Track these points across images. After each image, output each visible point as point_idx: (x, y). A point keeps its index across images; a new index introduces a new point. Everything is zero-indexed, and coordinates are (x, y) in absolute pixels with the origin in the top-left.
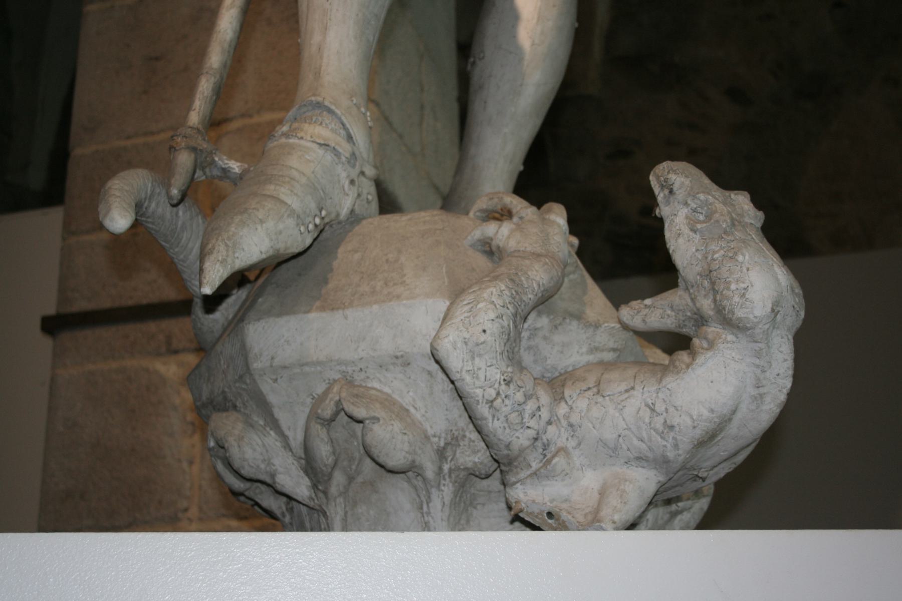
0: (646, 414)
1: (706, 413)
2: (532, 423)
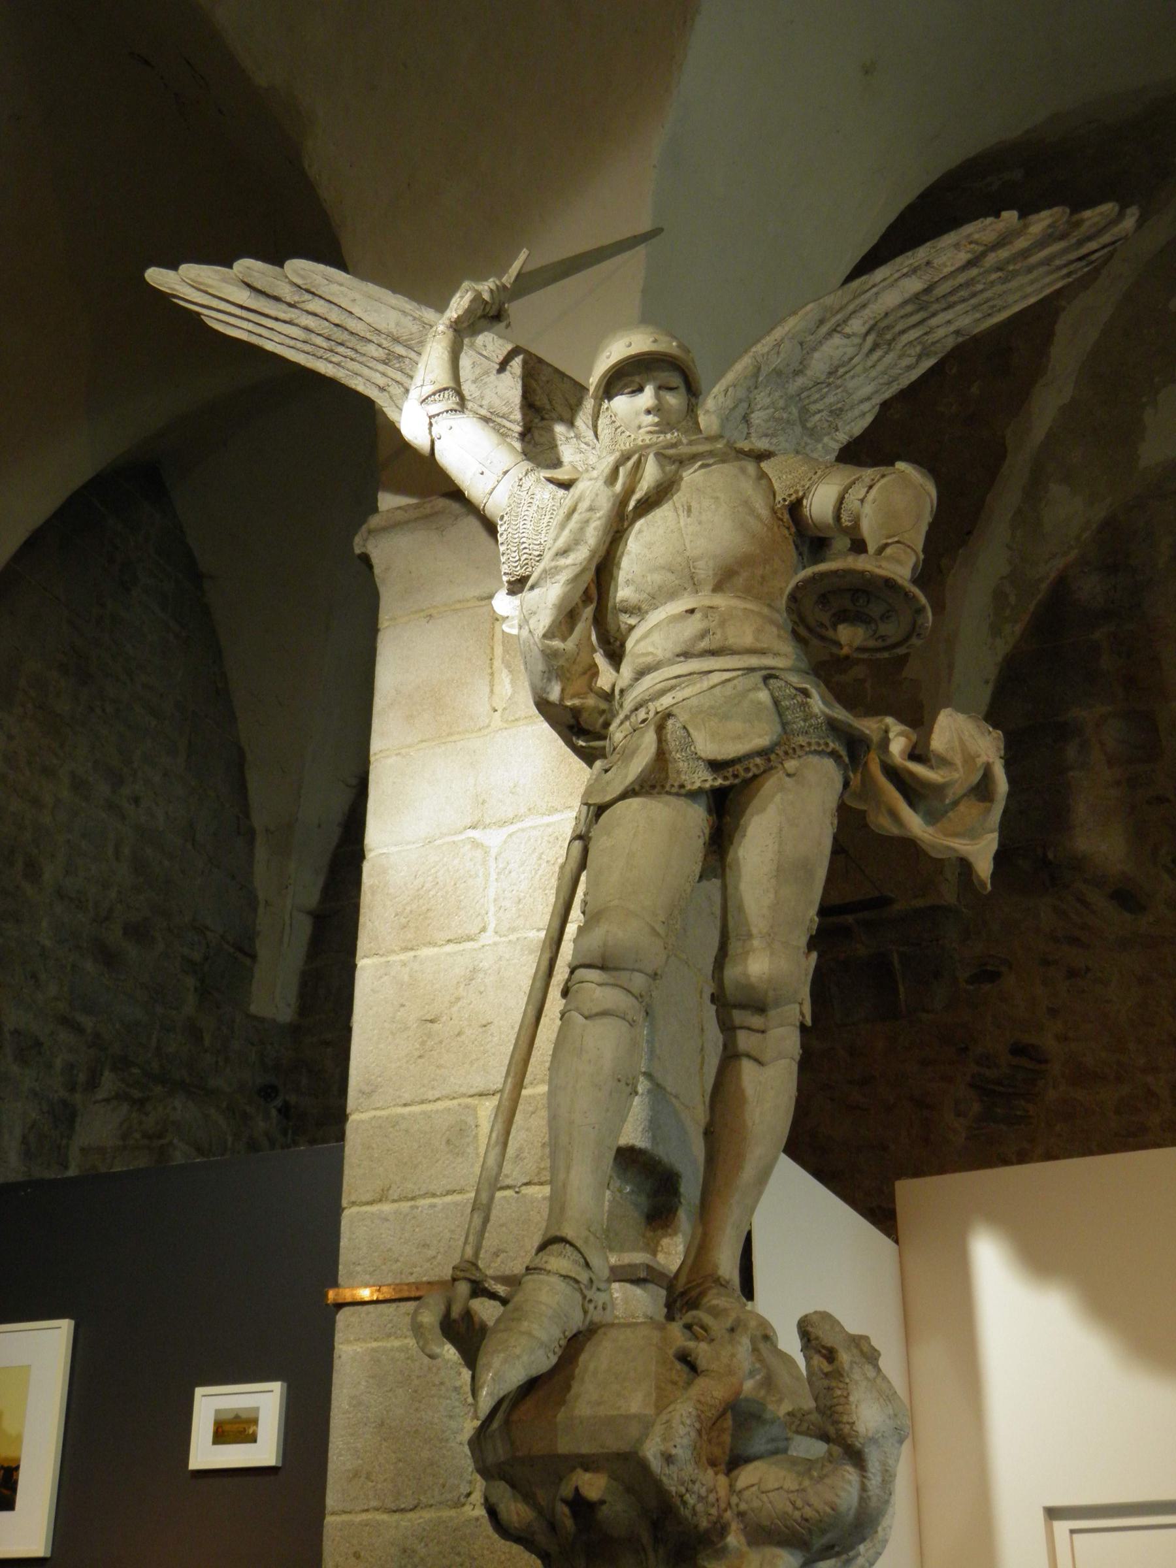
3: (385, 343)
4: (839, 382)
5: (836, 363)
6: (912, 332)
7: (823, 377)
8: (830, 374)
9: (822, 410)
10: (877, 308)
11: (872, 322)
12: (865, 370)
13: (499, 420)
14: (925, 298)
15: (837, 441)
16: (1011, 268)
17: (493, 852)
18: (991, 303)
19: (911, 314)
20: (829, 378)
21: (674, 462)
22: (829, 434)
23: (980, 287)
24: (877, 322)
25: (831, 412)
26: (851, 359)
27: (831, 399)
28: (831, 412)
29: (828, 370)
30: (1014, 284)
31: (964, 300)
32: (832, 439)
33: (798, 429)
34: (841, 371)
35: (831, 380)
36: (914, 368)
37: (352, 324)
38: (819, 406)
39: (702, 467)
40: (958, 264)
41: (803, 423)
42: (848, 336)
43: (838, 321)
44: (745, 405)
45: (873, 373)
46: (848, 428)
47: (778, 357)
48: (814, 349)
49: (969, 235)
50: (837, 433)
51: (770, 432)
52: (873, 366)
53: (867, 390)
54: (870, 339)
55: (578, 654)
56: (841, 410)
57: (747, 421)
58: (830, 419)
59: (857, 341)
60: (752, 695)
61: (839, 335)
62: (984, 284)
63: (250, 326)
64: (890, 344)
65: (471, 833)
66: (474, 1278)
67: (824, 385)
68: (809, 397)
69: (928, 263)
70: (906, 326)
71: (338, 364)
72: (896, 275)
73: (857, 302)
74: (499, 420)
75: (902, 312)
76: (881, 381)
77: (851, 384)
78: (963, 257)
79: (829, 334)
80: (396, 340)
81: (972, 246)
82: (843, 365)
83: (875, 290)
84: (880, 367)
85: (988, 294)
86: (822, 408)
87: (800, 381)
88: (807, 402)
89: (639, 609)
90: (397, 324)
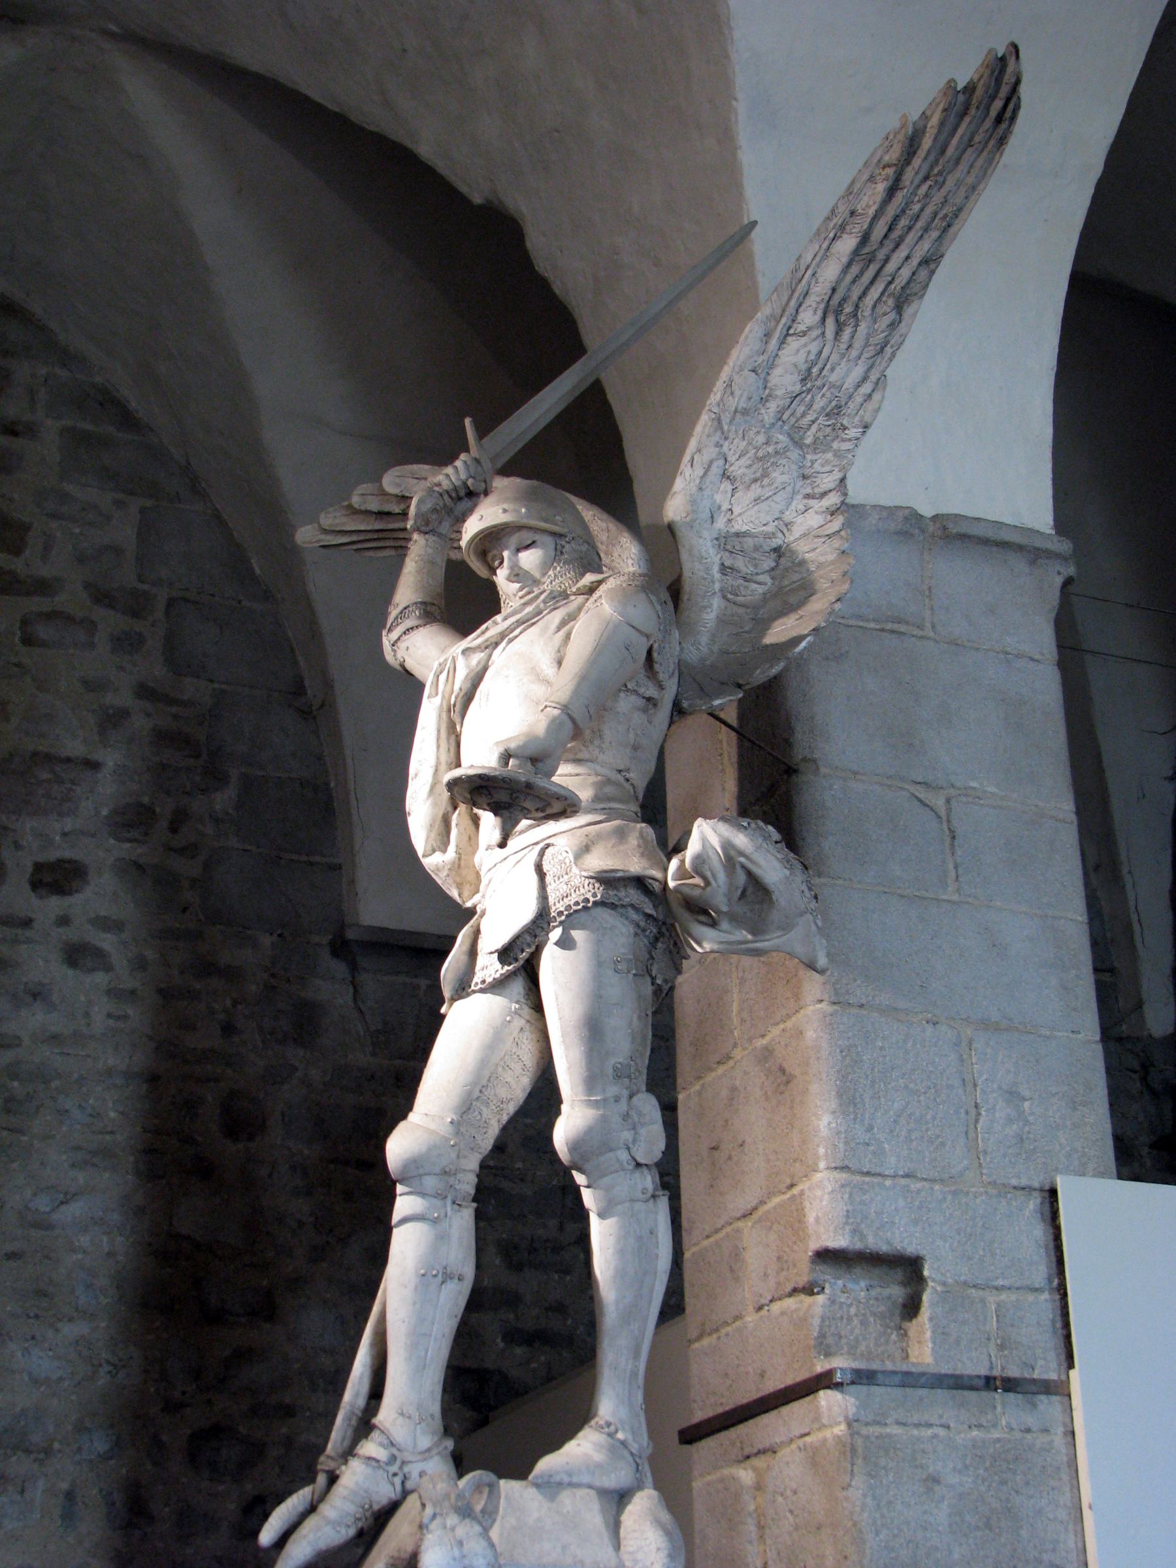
4: (819, 383)
5: (804, 367)
6: (872, 290)
7: (797, 388)
8: (804, 380)
9: (817, 419)
10: (820, 290)
11: (822, 306)
12: (843, 356)
14: (866, 250)
15: (850, 440)
16: (936, 171)
18: (940, 215)
19: (862, 273)
21: (486, 648)
22: (838, 437)
23: (916, 207)
24: (828, 301)
25: (827, 415)
26: (821, 352)
27: (819, 403)
28: (827, 415)
29: (800, 377)
30: (950, 183)
31: (910, 228)
32: (843, 440)
33: (794, 454)
34: (815, 370)
35: (809, 386)
36: (900, 322)
38: (809, 418)
39: (511, 641)
40: (879, 198)
41: (799, 444)
42: (804, 334)
43: (785, 324)
44: (721, 462)
45: (854, 353)
47: (734, 398)
48: (771, 366)
49: (879, 161)
50: (846, 432)
51: (758, 475)
52: (850, 346)
53: (858, 372)
54: (830, 322)
55: (460, 859)
56: (839, 407)
58: (829, 423)
61: (794, 338)
62: (919, 201)
63: (391, 543)
64: (855, 315)
66: (327, 1468)
67: (804, 395)
68: (792, 414)
69: (852, 213)
70: (862, 289)
72: (825, 246)
73: (796, 295)
75: (849, 278)
77: (833, 378)
78: (881, 187)
79: (782, 343)
82: (814, 364)
83: (809, 272)
84: (858, 344)
86: (815, 416)
87: (773, 406)
88: (793, 420)
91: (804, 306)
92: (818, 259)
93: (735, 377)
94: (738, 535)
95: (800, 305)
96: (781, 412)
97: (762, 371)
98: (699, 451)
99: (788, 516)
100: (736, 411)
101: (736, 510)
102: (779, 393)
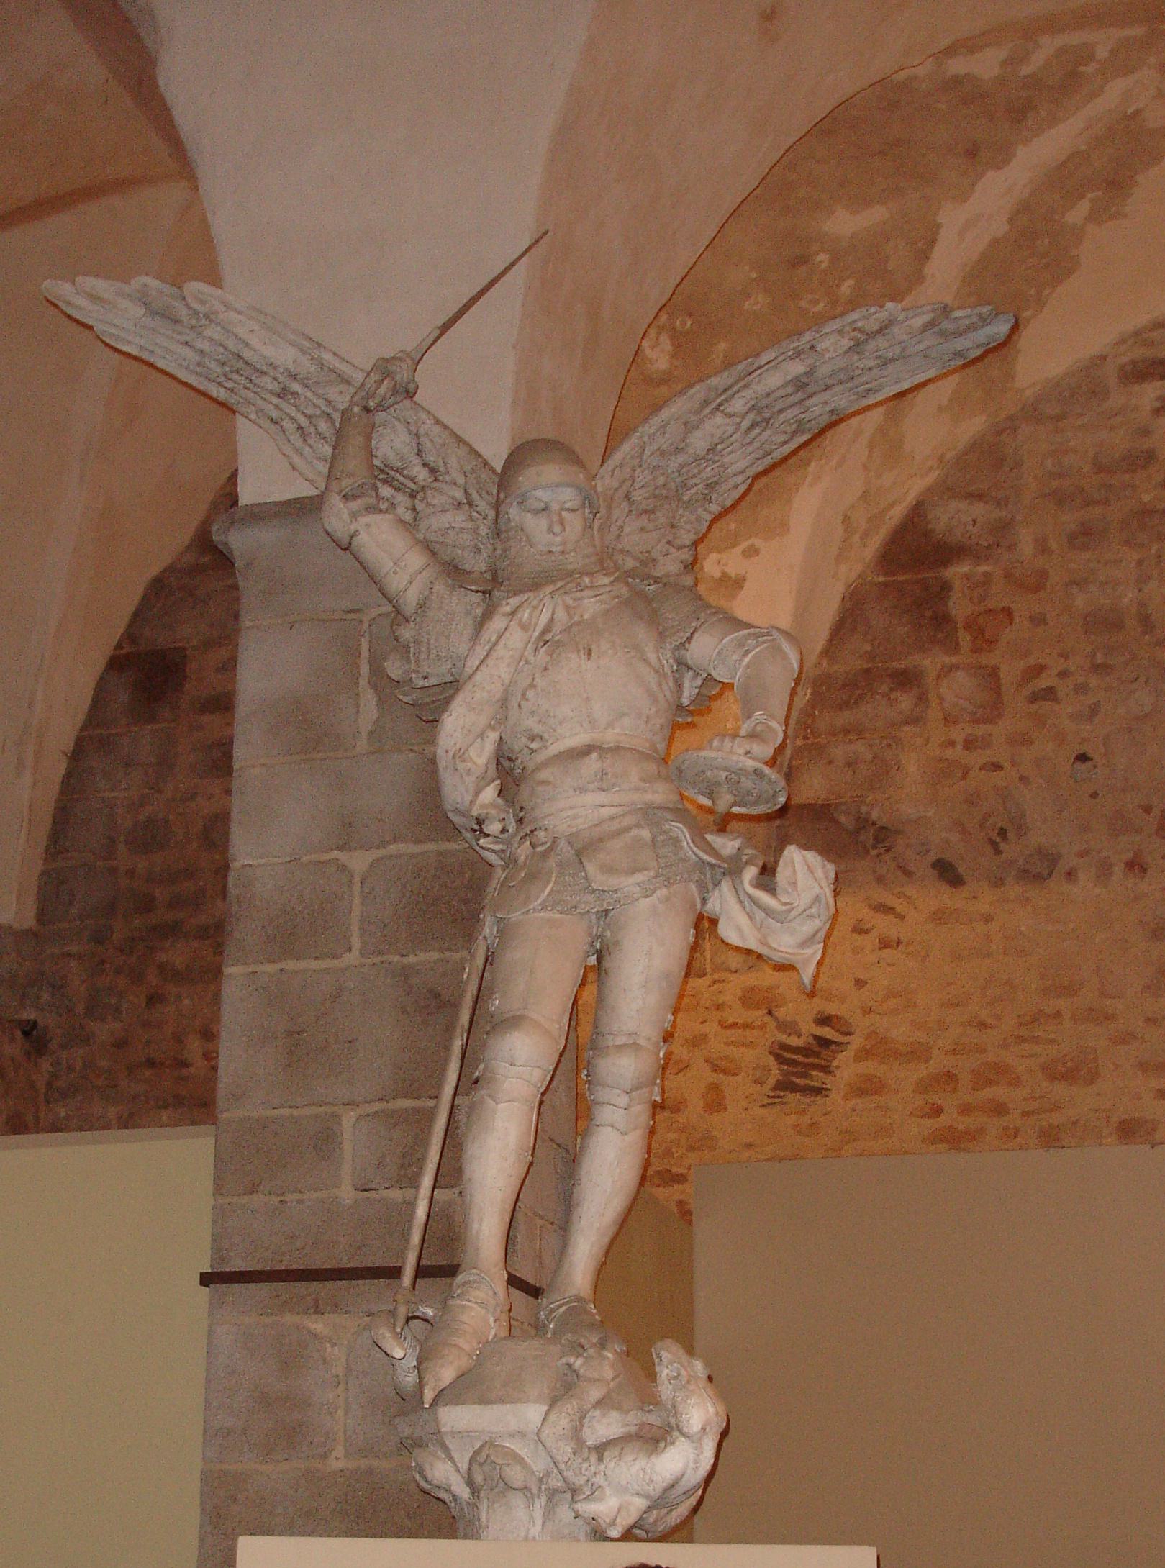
0: (641, 1474)
1: (668, 1476)
2: (587, 1473)
3: (281, 378)
4: (717, 458)
5: (716, 440)
12: (743, 446)
13: (392, 473)
15: (710, 512)
17: (357, 879)
18: (867, 386)
20: (707, 454)
32: (705, 510)
34: (719, 447)
35: (709, 456)
37: (247, 354)
38: (694, 481)
42: (730, 416)
45: (750, 449)
46: (721, 499)
48: (696, 427)
51: (649, 508)
54: (751, 416)
56: (716, 483)
57: (629, 499)
59: (738, 420)
60: (634, 832)
64: (768, 422)
65: (335, 854)
69: (812, 347)
71: (232, 390)
72: (780, 359)
73: (742, 384)
74: (392, 473)
76: (758, 456)
77: (726, 460)
79: (712, 413)
80: (294, 377)
81: (856, 333)
83: (759, 371)
84: (756, 444)
85: (864, 379)
86: (699, 481)
89: (541, 738)
90: (295, 361)
91: (740, 394)
92: (770, 365)
93: (672, 422)
94: (622, 551)
95: (738, 391)
96: (682, 466)
97: (689, 428)
98: (621, 466)
99: (655, 554)
100: (658, 449)
101: (627, 529)
102: (691, 451)
